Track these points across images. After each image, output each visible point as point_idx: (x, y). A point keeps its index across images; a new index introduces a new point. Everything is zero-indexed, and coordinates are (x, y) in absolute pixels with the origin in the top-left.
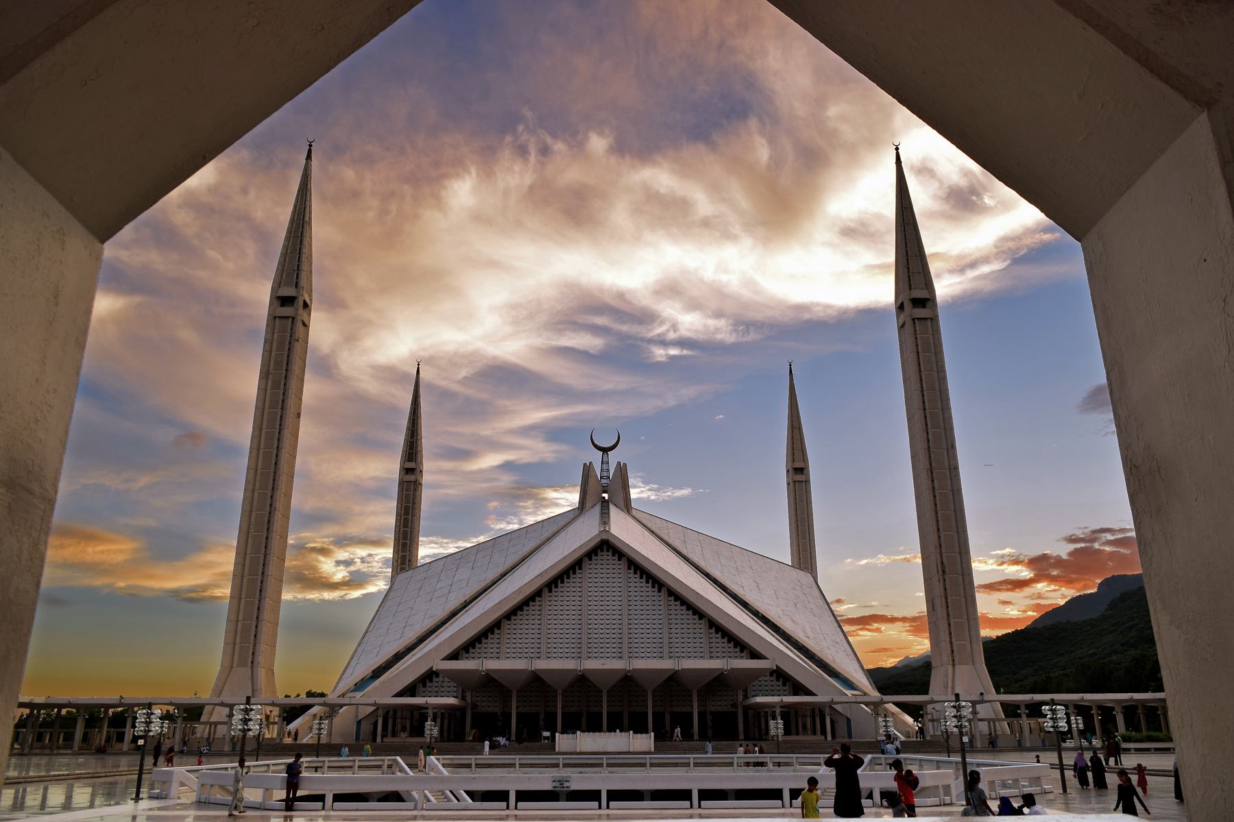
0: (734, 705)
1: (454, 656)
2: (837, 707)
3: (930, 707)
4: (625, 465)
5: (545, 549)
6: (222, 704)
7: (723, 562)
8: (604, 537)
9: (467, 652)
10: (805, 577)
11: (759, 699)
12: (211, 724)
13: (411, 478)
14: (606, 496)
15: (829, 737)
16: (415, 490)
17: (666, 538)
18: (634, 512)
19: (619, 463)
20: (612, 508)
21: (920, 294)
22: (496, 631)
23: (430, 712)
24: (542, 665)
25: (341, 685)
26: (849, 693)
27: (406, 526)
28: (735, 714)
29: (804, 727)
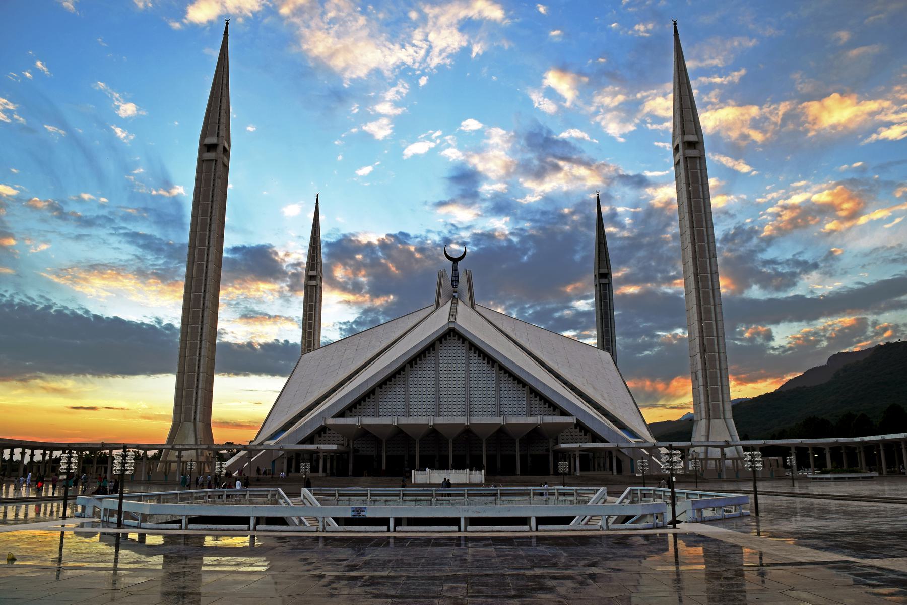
0: (547, 450)
2: (623, 450)
3: (691, 450)
8: (451, 326)
9: (351, 412)
10: (607, 356)
11: (563, 446)
15: (615, 473)
18: (477, 308)
21: (692, 138)
22: (372, 396)
23: (321, 455)
24: (404, 421)
26: (633, 440)
28: (548, 456)
29: (599, 465)
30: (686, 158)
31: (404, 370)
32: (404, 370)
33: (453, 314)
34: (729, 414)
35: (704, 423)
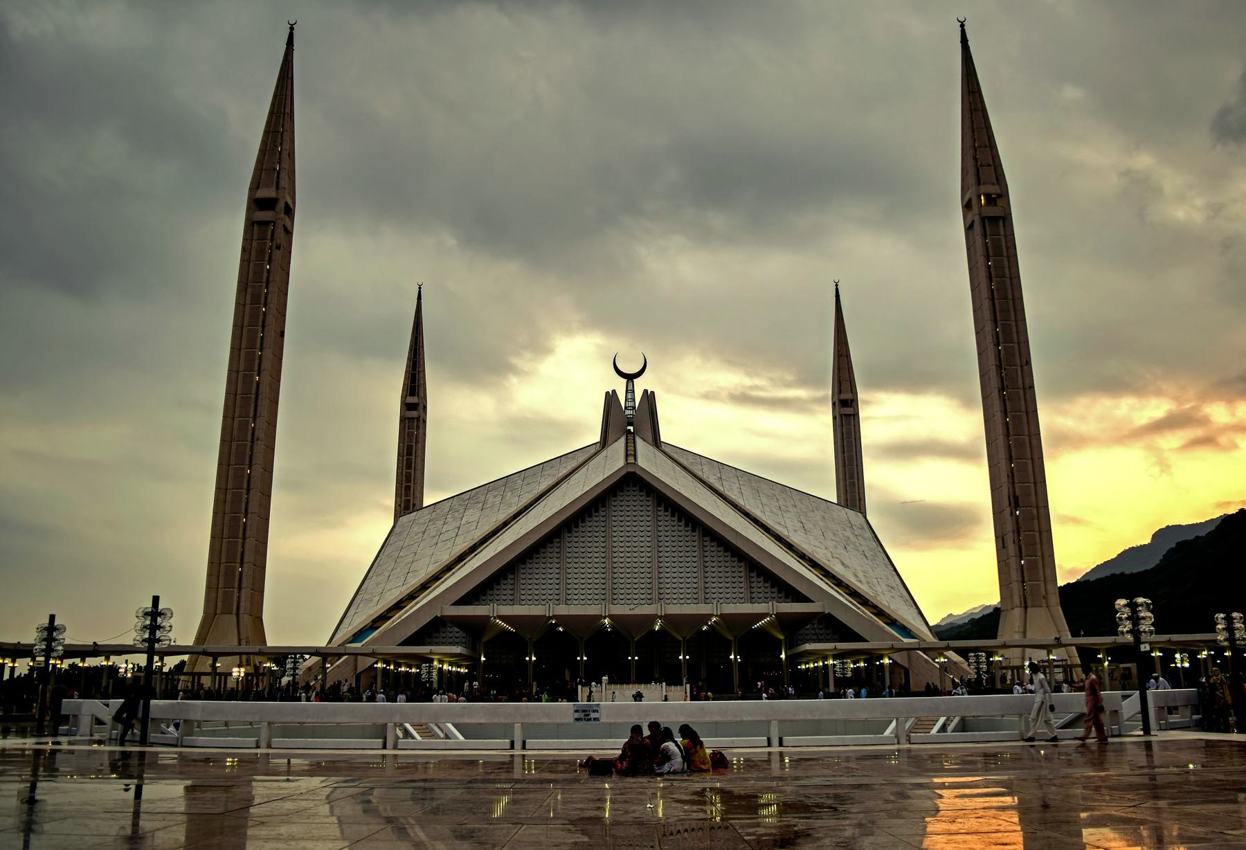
1: (463, 601)
4: (653, 393)
5: (564, 486)
6: (205, 653)
7: (764, 500)
8: (631, 469)
9: (478, 600)
11: (808, 647)
12: (193, 674)
13: (414, 414)
14: (631, 428)
16: (418, 427)
17: (700, 474)
19: (646, 391)
20: (638, 440)
25: (337, 637)
26: (905, 640)
27: (409, 466)
30: (983, 219)
31: (559, 537)
32: (559, 537)
33: (631, 453)
34: (1055, 600)
35: (1018, 612)
